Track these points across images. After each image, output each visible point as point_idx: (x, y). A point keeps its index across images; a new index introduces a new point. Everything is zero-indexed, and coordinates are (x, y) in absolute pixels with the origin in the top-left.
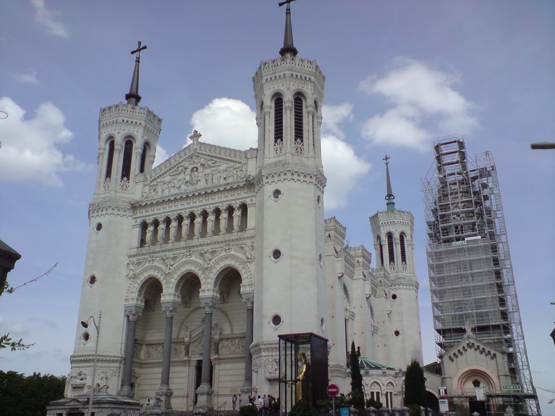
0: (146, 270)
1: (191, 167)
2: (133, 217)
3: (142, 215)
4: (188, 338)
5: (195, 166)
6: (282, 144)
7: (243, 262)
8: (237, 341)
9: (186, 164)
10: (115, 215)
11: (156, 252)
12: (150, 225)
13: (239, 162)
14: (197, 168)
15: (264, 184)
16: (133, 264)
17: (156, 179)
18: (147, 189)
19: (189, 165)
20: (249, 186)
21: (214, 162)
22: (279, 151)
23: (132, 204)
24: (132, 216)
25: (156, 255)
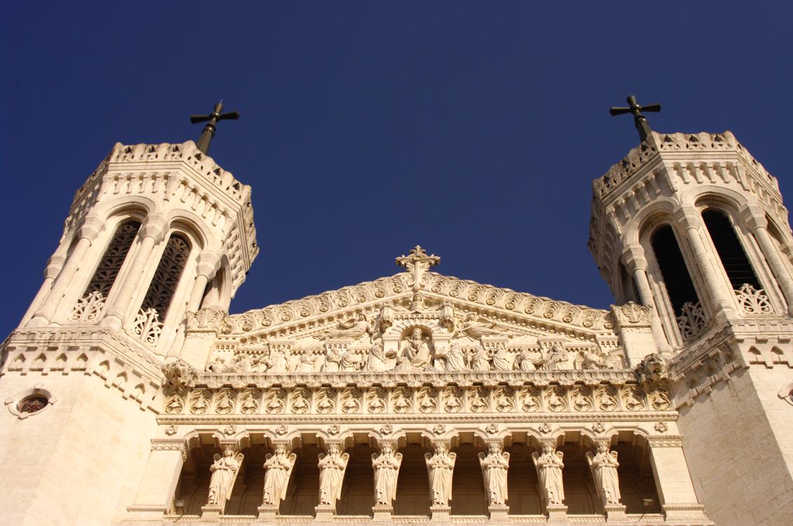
5: (418, 322)
6: (763, 293)
9: (389, 313)
10: (109, 383)
12: (229, 452)
13: (584, 336)
14: (426, 334)
15: (748, 364)
17: (263, 336)
18: (229, 356)
19: (397, 319)
21: (490, 325)
23: (177, 373)
24: (157, 413)
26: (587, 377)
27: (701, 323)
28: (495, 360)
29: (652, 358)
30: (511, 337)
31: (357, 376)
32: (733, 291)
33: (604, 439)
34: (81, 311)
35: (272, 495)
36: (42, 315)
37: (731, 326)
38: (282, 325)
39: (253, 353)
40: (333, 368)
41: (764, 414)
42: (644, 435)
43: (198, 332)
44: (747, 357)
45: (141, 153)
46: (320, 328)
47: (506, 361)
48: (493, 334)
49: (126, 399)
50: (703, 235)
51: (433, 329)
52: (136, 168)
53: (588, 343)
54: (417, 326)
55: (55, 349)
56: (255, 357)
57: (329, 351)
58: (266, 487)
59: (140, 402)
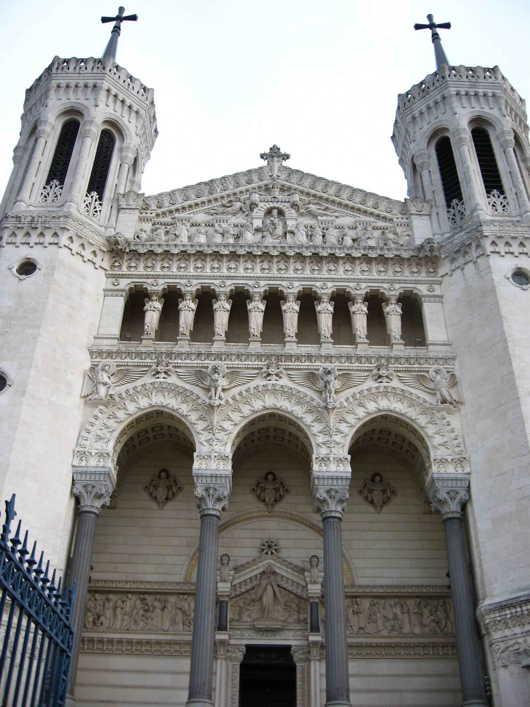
0: (145, 391)
1: (265, 205)
2: (107, 272)
3: (133, 272)
4: (229, 585)
5: (275, 205)
6: (505, 198)
7: (432, 409)
8: (366, 603)
9: (256, 197)
11: (179, 355)
12: (155, 298)
13: (385, 218)
14: (281, 213)
15: (489, 253)
16: (106, 371)
17: (171, 212)
18: (148, 226)
20: (423, 261)
21: (323, 208)
22: (500, 208)
23: (117, 243)
24: (106, 270)
25: (175, 361)
26: (386, 252)
27: (462, 216)
28: (326, 235)
29: (429, 241)
30: (337, 217)
31: (236, 246)
32: (486, 195)
33: (394, 295)
34: (47, 195)
35: (185, 328)
36: (22, 201)
37: (481, 226)
38: (183, 204)
39: (164, 224)
40: (218, 239)
41: (494, 289)
42: (420, 294)
43: (127, 209)
44: (489, 248)
45: (74, 65)
46: (209, 207)
47: (333, 236)
48: (326, 215)
49: (85, 262)
50: (471, 150)
51: (286, 210)
52: (72, 78)
53: (387, 224)
54: (275, 208)
55: (37, 228)
56: (166, 228)
57: (216, 225)
58: (180, 323)
59: (94, 264)
